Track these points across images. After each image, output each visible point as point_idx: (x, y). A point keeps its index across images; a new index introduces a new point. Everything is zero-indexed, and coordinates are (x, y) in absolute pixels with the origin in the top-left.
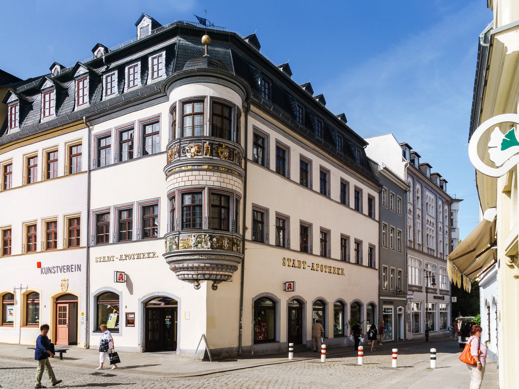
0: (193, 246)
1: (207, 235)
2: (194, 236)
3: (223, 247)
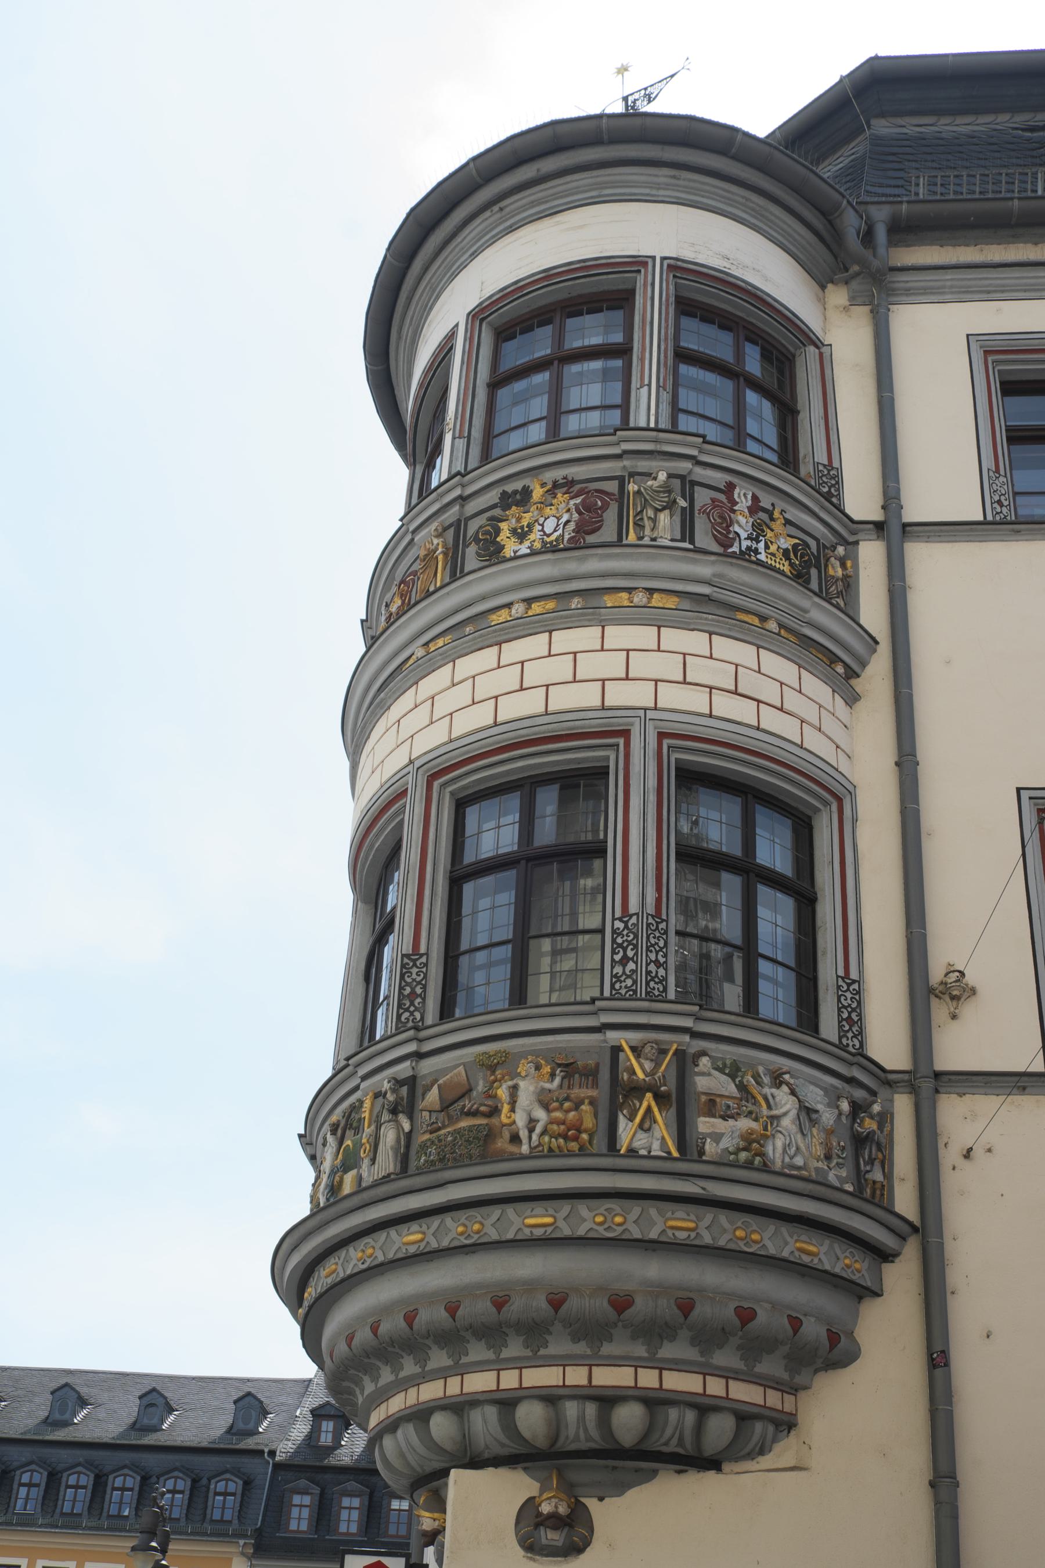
1: (386, 1086)
3: (502, 1143)
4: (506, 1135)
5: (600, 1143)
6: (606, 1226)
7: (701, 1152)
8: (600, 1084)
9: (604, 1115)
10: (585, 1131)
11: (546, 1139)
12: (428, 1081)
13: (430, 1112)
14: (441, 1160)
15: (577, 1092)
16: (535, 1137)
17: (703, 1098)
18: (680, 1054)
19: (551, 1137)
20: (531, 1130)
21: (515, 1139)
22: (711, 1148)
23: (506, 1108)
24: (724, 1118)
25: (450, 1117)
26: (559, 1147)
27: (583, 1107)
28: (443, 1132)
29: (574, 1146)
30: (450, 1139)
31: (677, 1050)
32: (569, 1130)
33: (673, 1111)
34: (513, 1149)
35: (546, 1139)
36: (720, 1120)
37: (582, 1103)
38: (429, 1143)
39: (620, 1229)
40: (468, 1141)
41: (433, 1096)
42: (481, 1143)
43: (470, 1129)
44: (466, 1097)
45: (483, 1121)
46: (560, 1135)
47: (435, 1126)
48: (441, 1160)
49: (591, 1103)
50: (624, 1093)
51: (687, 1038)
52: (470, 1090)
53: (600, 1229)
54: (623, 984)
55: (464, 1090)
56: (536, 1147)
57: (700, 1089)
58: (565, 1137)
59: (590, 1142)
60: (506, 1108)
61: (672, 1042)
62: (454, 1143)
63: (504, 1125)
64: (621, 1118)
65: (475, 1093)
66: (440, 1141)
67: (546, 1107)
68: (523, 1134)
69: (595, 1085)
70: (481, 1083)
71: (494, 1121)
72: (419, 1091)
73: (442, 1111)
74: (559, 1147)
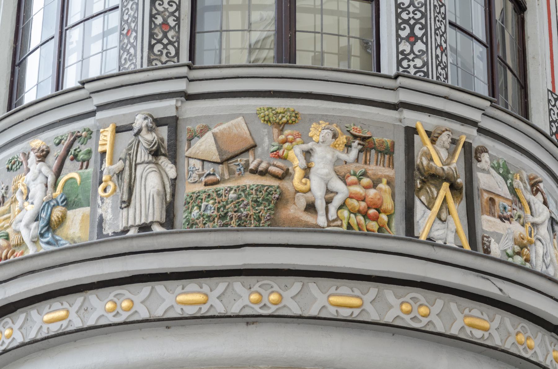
0: (26, 236)
1: (139, 122)
2: (43, 156)
3: (295, 210)
4: (302, 202)
5: (398, 227)
6: (412, 315)
7: (487, 251)
8: (396, 164)
9: (401, 198)
10: (385, 212)
11: (345, 213)
12: (197, 127)
13: (203, 161)
14: (223, 217)
15: (372, 168)
16: (333, 209)
17: (486, 196)
18: (467, 146)
19: (351, 213)
20: (328, 202)
21: (311, 208)
22: (496, 250)
23: (298, 174)
24: (502, 218)
25: (231, 172)
26: (358, 224)
27: (380, 186)
29: (373, 226)
30: (232, 195)
31: (465, 142)
32: (369, 208)
33: (464, 202)
34: (308, 218)
35: (345, 213)
36: (498, 221)
37: (379, 181)
38: (204, 196)
39: (425, 321)
40: (256, 201)
41: (205, 145)
42: (272, 205)
43: (259, 189)
44: (251, 152)
45: (275, 183)
46: (359, 212)
47: (211, 178)
48: (223, 217)
49: (388, 183)
50: (419, 179)
51: (473, 131)
52: (254, 146)
53: (407, 318)
54: (412, 64)
55: (247, 145)
56: (334, 221)
57: (482, 186)
58: (365, 215)
59: (389, 224)
60: (298, 174)
61: (463, 133)
62: (238, 201)
63: (297, 192)
64: (417, 202)
65: (259, 150)
66: (219, 195)
67: (343, 178)
68: (320, 204)
69: (391, 164)
70: (266, 140)
71: (285, 184)
72: (183, 136)
73: (221, 163)
74: (358, 224)
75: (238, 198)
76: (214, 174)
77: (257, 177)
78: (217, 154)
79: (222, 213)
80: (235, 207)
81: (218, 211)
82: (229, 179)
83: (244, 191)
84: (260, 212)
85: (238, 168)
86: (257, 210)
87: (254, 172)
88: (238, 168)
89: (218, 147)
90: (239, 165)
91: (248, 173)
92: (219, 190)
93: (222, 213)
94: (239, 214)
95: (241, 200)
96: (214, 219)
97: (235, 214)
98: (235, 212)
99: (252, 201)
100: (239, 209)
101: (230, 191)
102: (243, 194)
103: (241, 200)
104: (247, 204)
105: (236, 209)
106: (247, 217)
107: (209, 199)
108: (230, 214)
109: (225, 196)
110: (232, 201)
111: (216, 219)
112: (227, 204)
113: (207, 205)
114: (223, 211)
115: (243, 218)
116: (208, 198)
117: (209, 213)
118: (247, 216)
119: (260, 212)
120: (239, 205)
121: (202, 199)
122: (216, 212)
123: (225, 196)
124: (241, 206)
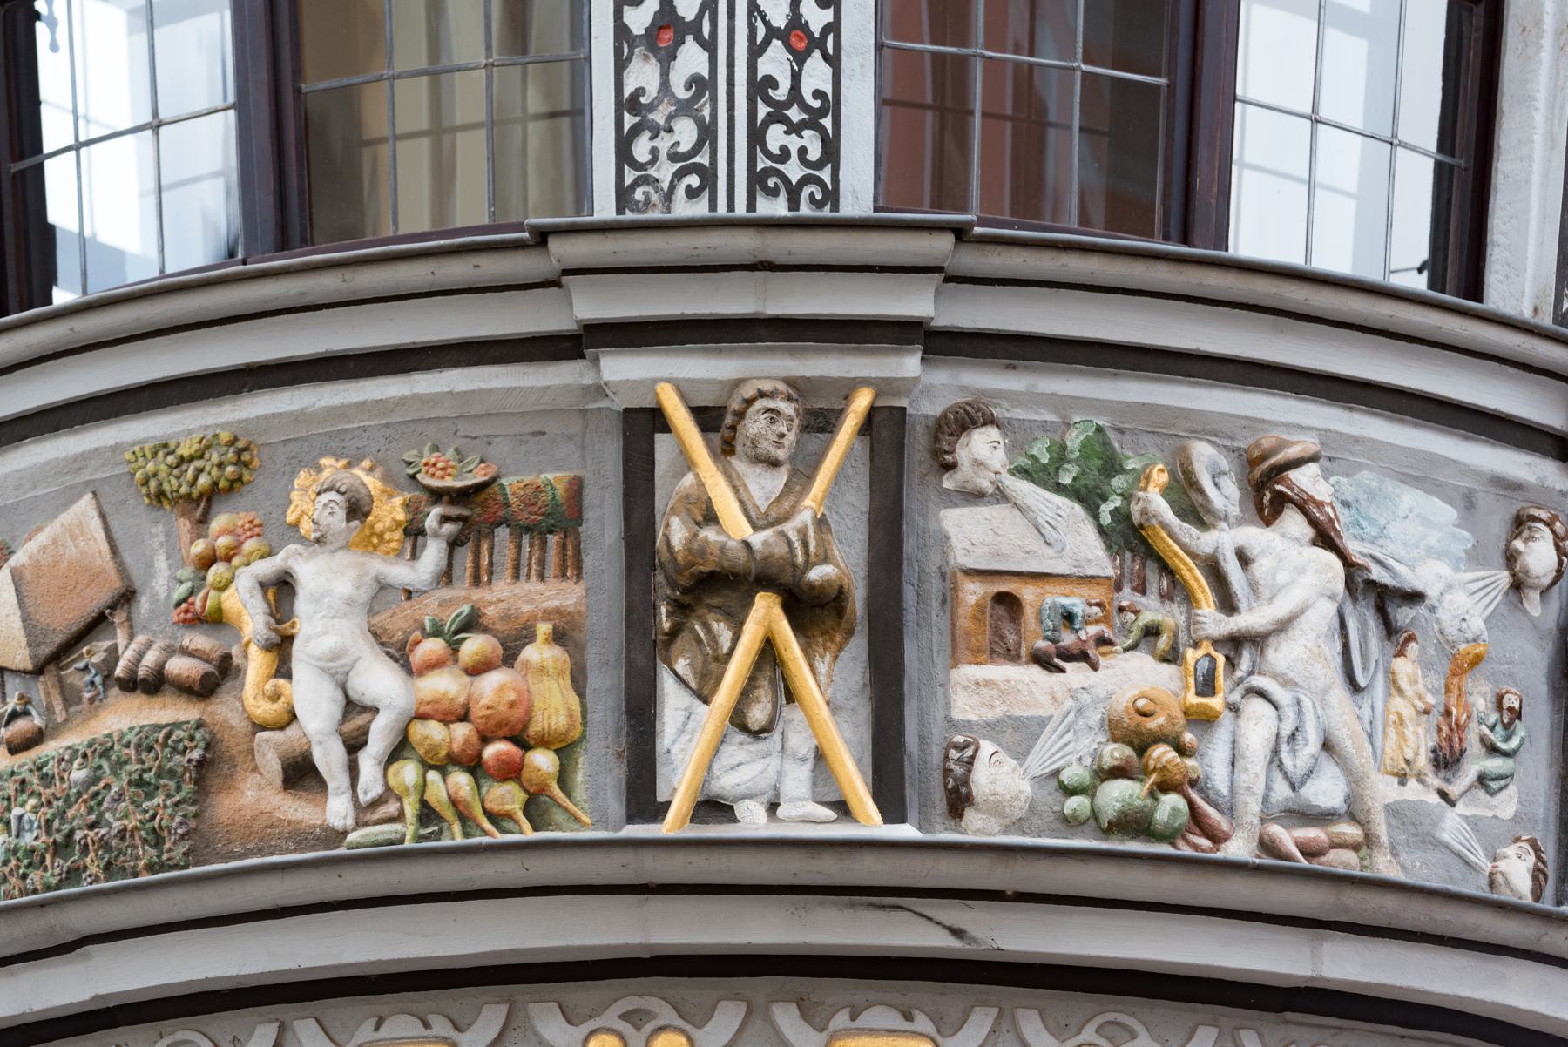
3: (255, 794)
8: (589, 561)
9: (606, 682)
10: (544, 742)
14: (62, 847)
19: (427, 766)
20: (354, 745)
21: (301, 774)
23: (256, 664)
25: (70, 698)
28: (50, 749)
30: (78, 775)
32: (485, 740)
34: (297, 810)
35: (408, 772)
37: (525, 635)
40: (140, 783)
42: (188, 788)
47: (21, 725)
49: (559, 637)
52: (127, 597)
56: (376, 804)
58: (474, 766)
59: (563, 779)
60: (256, 664)
62: (92, 793)
65: (144, 605)
66: (47, 780)
67: (400, 654)
68: (329, 758)
69: (572, 565)
70: (161, 563)
71: (224, 711)
73: (38, 671)
74: (454, 802)
75: (95, 780)
76: (26, 713)
77: (138, 699)
78: (24, 641)
79: (59, 837)
80: (90, 810)
81: (48, 833)
82: (66, 720)
83: (105, 754)
84: (153, 818)
85: (88, 678)
86: (146, 812)
87: (130, 684)
88: (88, 678)
89: (26, 619)
90: (86, 669)
91: (115, 691)
92: (45, 764)
93: (59, 837)
94: (103, 831)
95: (102, 784)
96: (43, 860)
97: (91, 834)
98: (91, 827)
99: (130, 783)
100: (101, 814)
101: (71, 761)
102: (106, 765)
103: (102, 784)
104: (119, 798)
105: (93, 817)
106: (123, 839)
107: (24, 796)
108: (78, 835)
109: (62, 779)
110: (79, 794)
111: (48, 858)
112: (68, 803)
113: (20, 818)
114: (58, 831)
115: (114, 842)
116: (23, 791)
117: (28, 839)
118: (122, 834)
119: (153, 818)
120: (100, 804)
121: (9, 799)
122: (44, 838)
123: (62, 779)
124: (105, 805)
